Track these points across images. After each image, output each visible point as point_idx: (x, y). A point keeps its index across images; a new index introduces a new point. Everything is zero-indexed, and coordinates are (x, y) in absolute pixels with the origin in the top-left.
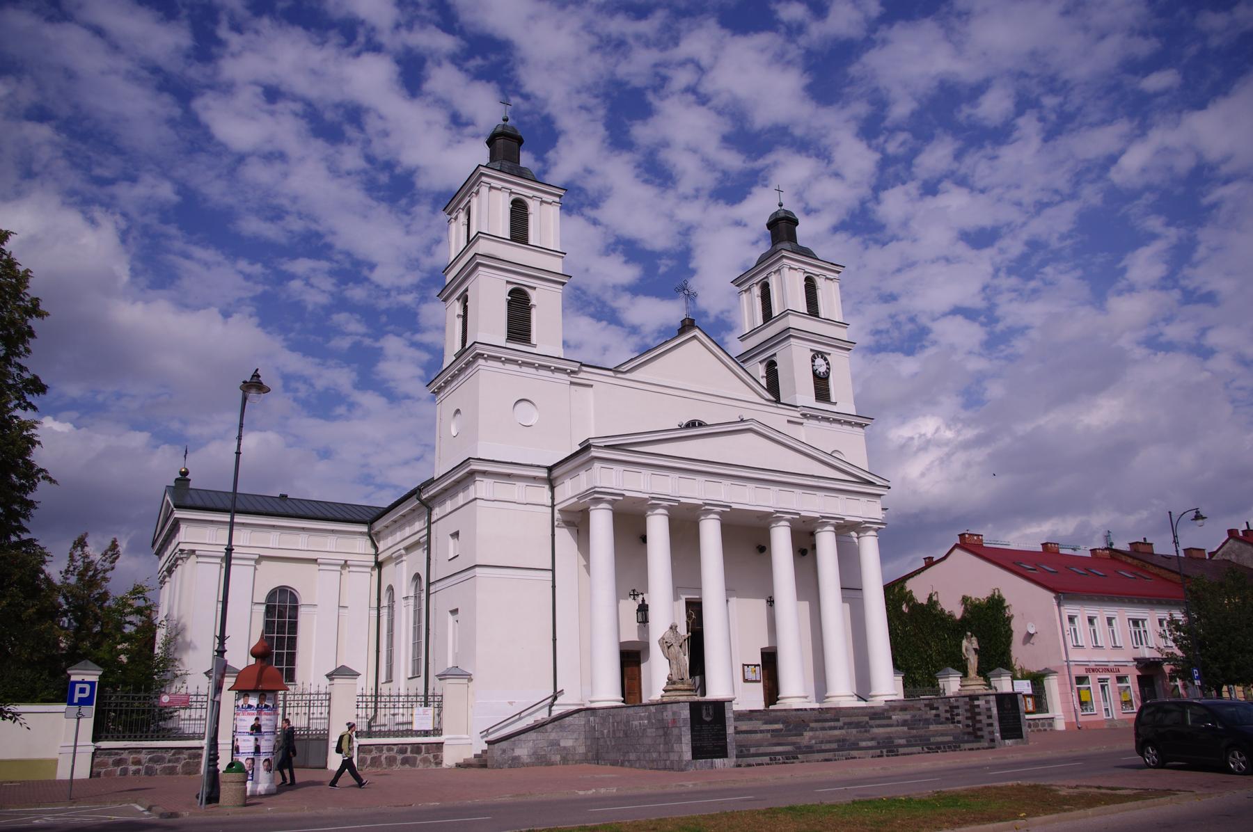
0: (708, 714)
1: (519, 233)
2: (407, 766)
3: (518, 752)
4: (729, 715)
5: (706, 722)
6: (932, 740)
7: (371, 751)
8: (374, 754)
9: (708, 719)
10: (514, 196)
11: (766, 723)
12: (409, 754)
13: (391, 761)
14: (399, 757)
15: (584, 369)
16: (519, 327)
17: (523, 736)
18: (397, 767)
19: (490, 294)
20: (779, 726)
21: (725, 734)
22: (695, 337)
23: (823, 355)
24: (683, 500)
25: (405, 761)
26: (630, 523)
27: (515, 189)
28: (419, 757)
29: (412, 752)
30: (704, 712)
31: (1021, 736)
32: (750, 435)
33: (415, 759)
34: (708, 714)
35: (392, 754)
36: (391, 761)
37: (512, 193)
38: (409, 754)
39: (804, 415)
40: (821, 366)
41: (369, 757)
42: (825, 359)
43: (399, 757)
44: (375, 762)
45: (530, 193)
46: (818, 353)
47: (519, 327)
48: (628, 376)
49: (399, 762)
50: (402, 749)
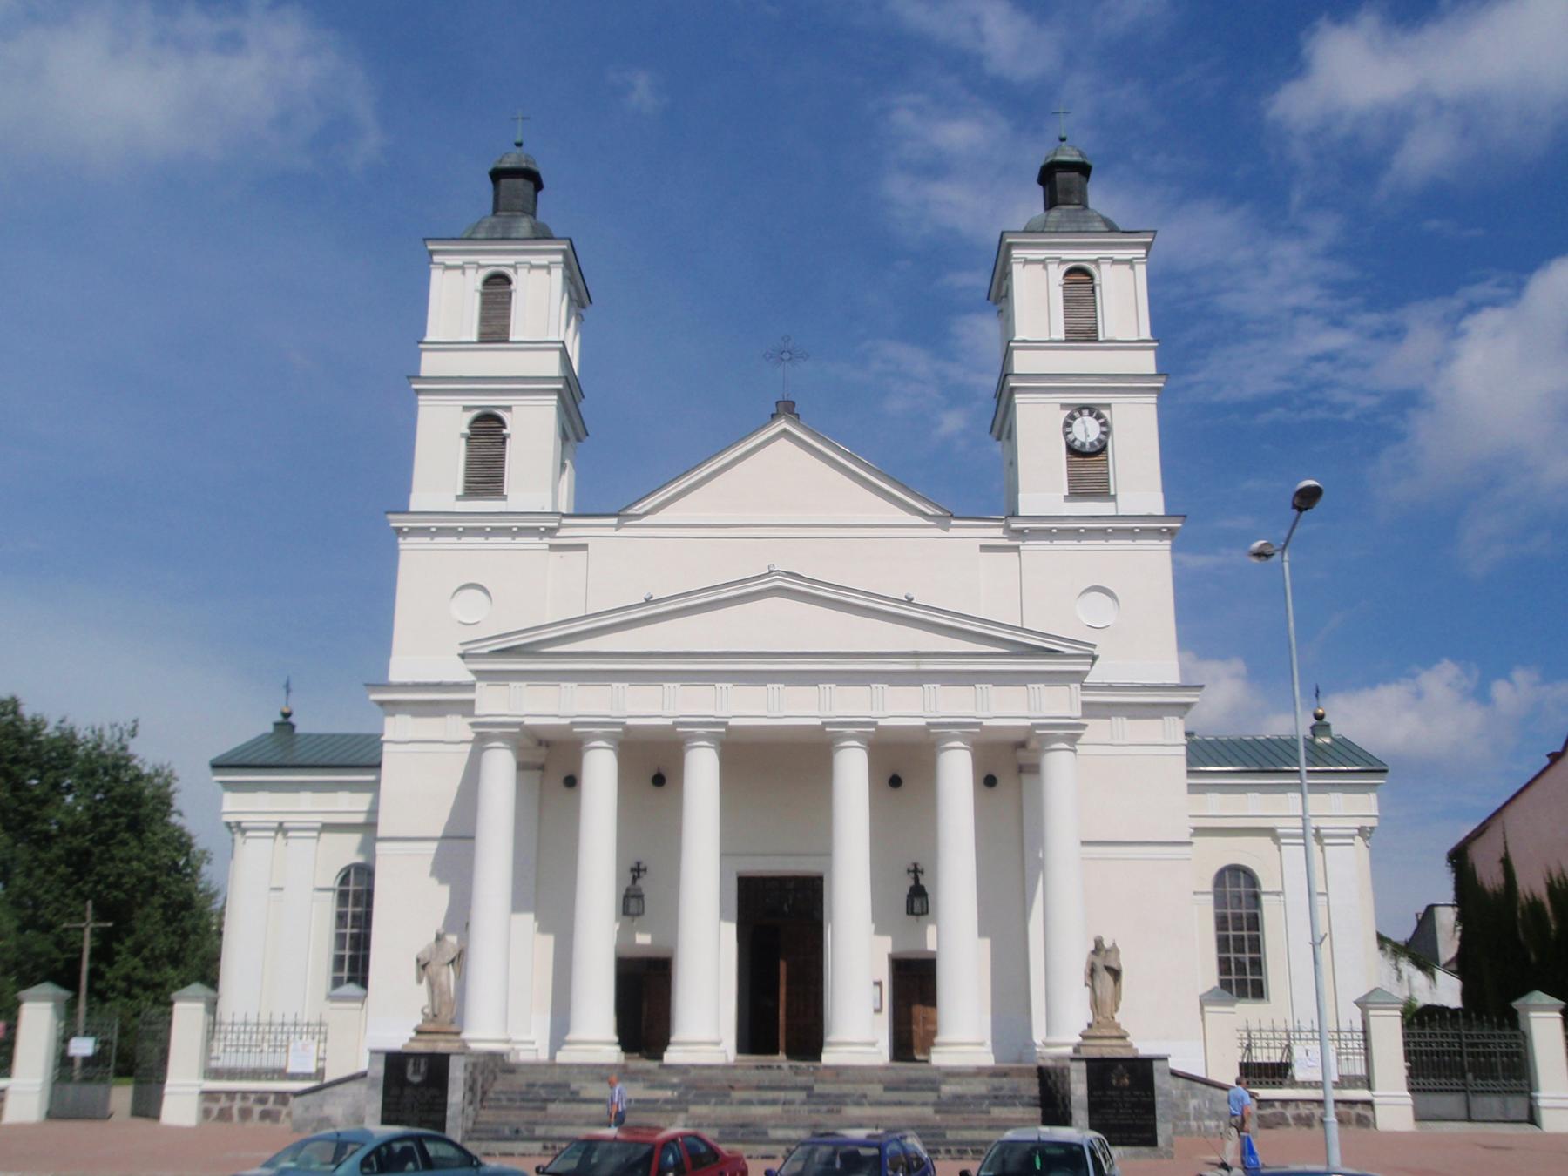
0: (416, 1072)
1: (494, 329)
2: (268, 1123)
4: (457, 1074)
5: (410, 1084)
6: (950, 1135)
7: (217, 1100)
8: (224, 1103)
9: (416, 1079)
10: (483, 274)
11: (652, 1087)
12: (270, 1105)
13: (245, 1114)
14: (258, 1109)
15: (565, 521)
16: (485, 474)
17: (338, 1088)
19: (440, 435)
20: (669, 1094)
21: (445, 1105)
22: (785, 433)
23: (1092, 410)
24: (630, 722)
25: (265, 1115)
26: (551, 762)
27: (483, 260)
28: (284, 1110)
30: (410, 1068)
31: (1152, 1142)
32: (775, 602)
33: (279, 1113)
34: (416, 1072)
36: (245, 1114)
37: (481, 267)
39: (1021, 531)
40: (1086, 432)
41: (215, 1108)
42: (1098, 417)
43: (258, 1109)
44: (224, 1115)
45: (510, 260)
46: (1081, 408)
47: (485, 474)
48: (643, 521)
49: (256, 1115)
50: (262, 1097)
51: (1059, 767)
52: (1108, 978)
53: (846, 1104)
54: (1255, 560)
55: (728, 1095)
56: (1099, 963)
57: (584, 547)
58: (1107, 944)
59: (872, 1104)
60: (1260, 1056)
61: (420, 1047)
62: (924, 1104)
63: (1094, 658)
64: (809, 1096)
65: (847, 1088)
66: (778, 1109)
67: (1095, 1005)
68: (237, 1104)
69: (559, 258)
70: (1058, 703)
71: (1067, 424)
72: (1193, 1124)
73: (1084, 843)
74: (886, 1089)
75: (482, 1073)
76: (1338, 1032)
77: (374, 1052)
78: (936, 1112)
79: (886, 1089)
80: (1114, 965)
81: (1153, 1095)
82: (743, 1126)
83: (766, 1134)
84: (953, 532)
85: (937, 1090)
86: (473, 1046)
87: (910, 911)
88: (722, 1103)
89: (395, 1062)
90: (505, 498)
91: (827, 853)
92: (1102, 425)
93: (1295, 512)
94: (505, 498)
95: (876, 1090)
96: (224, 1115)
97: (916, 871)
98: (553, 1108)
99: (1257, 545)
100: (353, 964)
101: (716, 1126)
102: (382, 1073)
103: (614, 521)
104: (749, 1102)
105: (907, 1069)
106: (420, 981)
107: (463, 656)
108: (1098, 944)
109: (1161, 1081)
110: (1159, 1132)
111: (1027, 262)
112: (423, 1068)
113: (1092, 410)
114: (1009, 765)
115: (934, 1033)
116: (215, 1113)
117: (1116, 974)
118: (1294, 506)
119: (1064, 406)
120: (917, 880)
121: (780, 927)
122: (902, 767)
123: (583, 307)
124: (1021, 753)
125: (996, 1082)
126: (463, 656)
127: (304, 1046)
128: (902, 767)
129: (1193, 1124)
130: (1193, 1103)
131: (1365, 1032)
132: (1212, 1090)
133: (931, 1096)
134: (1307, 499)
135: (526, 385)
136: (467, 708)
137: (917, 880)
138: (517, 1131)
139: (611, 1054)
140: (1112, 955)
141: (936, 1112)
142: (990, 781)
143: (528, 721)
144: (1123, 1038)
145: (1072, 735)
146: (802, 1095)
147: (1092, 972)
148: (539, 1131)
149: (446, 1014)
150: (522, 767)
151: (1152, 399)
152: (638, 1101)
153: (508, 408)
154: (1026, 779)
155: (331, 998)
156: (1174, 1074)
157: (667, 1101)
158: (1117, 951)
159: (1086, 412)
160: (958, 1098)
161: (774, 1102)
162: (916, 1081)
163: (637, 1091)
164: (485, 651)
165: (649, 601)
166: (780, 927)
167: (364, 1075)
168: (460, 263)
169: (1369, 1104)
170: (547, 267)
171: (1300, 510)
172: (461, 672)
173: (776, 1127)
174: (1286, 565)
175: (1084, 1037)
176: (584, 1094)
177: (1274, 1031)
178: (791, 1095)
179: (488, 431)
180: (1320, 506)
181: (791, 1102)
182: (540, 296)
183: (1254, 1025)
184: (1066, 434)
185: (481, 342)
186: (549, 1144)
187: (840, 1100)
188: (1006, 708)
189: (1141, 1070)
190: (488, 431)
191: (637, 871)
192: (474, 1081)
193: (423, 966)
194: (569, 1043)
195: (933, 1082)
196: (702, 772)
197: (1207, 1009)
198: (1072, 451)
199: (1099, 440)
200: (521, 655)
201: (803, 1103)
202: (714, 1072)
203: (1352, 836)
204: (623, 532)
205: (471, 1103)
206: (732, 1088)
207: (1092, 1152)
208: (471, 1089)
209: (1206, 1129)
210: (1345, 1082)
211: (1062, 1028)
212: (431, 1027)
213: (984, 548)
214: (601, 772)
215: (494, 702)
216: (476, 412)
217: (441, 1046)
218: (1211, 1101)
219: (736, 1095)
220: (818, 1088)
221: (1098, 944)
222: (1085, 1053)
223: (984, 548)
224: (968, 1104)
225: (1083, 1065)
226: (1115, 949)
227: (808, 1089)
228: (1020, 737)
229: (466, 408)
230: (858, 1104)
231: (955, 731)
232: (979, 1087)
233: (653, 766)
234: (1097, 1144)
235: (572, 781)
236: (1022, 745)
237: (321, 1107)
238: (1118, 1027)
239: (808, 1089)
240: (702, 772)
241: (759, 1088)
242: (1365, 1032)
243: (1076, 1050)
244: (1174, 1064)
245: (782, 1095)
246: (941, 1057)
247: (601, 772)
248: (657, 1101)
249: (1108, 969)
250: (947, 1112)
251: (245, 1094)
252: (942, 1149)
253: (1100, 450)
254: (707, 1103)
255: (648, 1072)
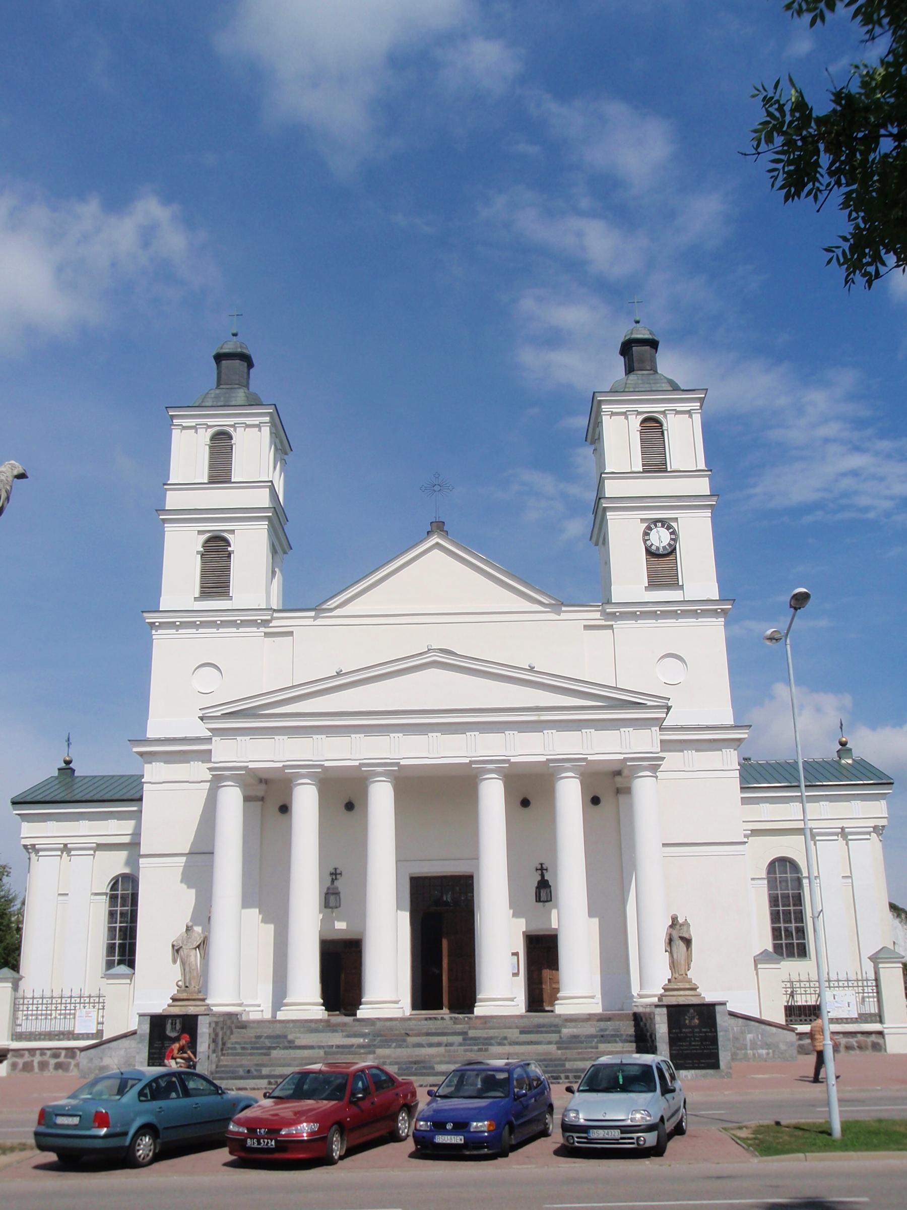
0: (173, 1029)
1: (220, 472)
2: (60, 1071)
3: (107, 1061)
4: (204, 1029)
6: (568, 1065)
8: (27, 1057)
10: (211, 432)
11: (348, 1036)
12: (62, 1059)
13: (43, 1066)
14: (53, 1061)
15: (275, 615)
16: (216, 582)
18: (50, 1072)
19: (182, 552)
22: (437, 543)
23: (664, 523)
24: (327, 764)
25: (58, 1066)
26: (269, 795)
27: (211, 422)
28: (73, 1062)
29: (66, 1056)
30: (169, 1027)
31: (715, 1066)
33: (69, 1064)
35: (46, 1058)
36: (43, 1066)
38: (62, 1059)
40: (660, 538)
42: (668, 528)
43: (53, 1061)
44: (28, 1067)
46: (656, 522)
47: (216, 582)
49: (51, 1067)
50: (56, 1052)
51: (645, 789)
52: (682, 945)
53: (491, 1044)
54: (768, 643)
55: (405, 1041)
56: (675, 935)
57: (291, 634)
58: (681, 920)
59: (510, 1044)
60: (801, 1000)
61: (176, 1011)
62: (550, 1043)
63: (669, 708)
64: (464, 1039)
65: (492, 1033)
66: (442, 1050)
67: (673, 965)
68: (37, 1059)
69: (267, 419)
70: (643, 742)
71: (646, 534)
72: (750, 1052)
73: (664, 845)
74: (521, 1032)
75: (222, 1028)
76: (829, 981)
77: (141, 1015)
78: (559, 1048)
79: (521, 1032)
80: (686, 935)
81: (716, 1031)
82: (415, 1063)
83: (433, 1068)
84: (563, 616)
85: (559, 1032)
86: (215, 1009)
87: (538, 899)
88: (400, 1046)
89: (158, 1023)
90: (231, 598)
91: (475, 857)
92: (671, 533)
93: (792, 610)
94: (231, 598)
95: (514, 1034)
96: (28, 1067)
97: (542, 869)
98: (274, 1053)
99: (769, 632)
100: (123, 950)
101: (397, 1063)
102: (148, 1031)
103: (312, 614)
104: (420, 1045)
105: (538, 1018)
106: (175, 961)
107: (202, 718)
108: (674, 919)
109: (722, 1021)
110: (721, 1058)
111: (613, 414)
112: (178, 1026)
113: (664, 523)
114: (608, 789)
115: (557, 990)
116: (21, 1066)
117: (688, 942)
118: (791, 606)
119: (643, 520)
120: (542, 876)
121: (442, 915)
122: (529, 793)
123: (286, 454)
124: (618, 779)
125: (603, 1024)
126: (202, 718)
127: (87, 1013)
128: (529, 793)
129: (750, 1052)
130: (749, 1036)
131: (877, 980)
132: (763, 1026)
133: (554, 1037)
134: (800, 600)
135: (245, 514)
136: (205, 756)
137: (542, 876)
138: (249, 1071)
139: (319, 1012)
140: (685, 928)
141: (559, 1048)
142: (595, 801)
143: (251, 765)
144: (694, 989)
145: (654, 765)
146: (459, 1039)
147: (670, 941)
148: (265, 1071)
149: (194, 986)
150: (247, 799)
151: (708, 513)
152: (338, 1047)
153: (232, 532)
154: (622, 798)
155: (107, 976)
156: (733, 1015)
157: (360, 1046)
158: (689, 925)
159: (659, 524)
160: (575, 1038)
161: (439, 1045)
162: (544, 1026)
163: (337, 1039)
164: (219, 714)
165: (339, 674)
166: (442, 915)
167: (134, 1033)
168: (194, 424)
169: (880, 1033)
170: (258, 426)
171: (796, 609)
172: (201, 730)
173: (441, 1063)
174: (788, 647)
175: (666, 990)
176: (298, 1043)
177: (809, 981)
178: (451, 1039)
179: (217, 549)
180: (810, 604)
181: (451, 1045)
182: (253, 449)
183: (795, 978)
184: (645, 541)
185: (210, 483)
186: (272, 1080)
187: (487, 1042)
188: (606, 746)
189: (707, 1013)
190: (217, 549)
191: (335, 875)
192: (217, 1035)
193: (177, 950)
194: (286, 1005)
195: (556, 1026)
196: (382, 799)
197: (759, 966)
198: (650, 553)
199: (669, 544)
200: (245, 717)
201: (460, 1045)
202: (394, 1023)
203: (869, 833)
204: (319, 622)
205: (214, 1051)
206: (408, 1035)
207: (660, 1070)
208: (214, 1041)
209: (760, 1056)
210: (864, 1018)
211: (650, 983)
212: (184, 995)
213: (586, 627)
214: (306, 801)
215: (227, 752)
216: (208, 535)
217: (192, 1010)
218: (762, 1035)
219: (411, 1040)
220: (472, 1033)
221: (674, 919)
222: (666, 1001)
223: (586, 627)
224: (582, 1042)
225: (665, 1010)
226: (686, 924)
227: (464, 1034)
228: (617, 768)
229: (200, 532)
230: (500, 1044)
231: (567, 765)
232: (590, 1029)
233: (345, 796)
234: (664, 1067)
235: (285, 809)
236: (619, 773)
237: (101, 1059)
238: (690, 981)
239: (464, 1034)
240: (382, 799)
241: (428, 1034)
242: (877, 980)
243: (660, 1000)
244: (730, 1007)
245: (444, 1039)
246: (561, 1008)
247: (306, 801)
248: (352, 1046)
249: (682, 938)
250: (566, 1048)
251: (42, 1051)
252: (563, 1075)
253: (671, 552)
254: (390, 1047)
255: (345, 1024)
